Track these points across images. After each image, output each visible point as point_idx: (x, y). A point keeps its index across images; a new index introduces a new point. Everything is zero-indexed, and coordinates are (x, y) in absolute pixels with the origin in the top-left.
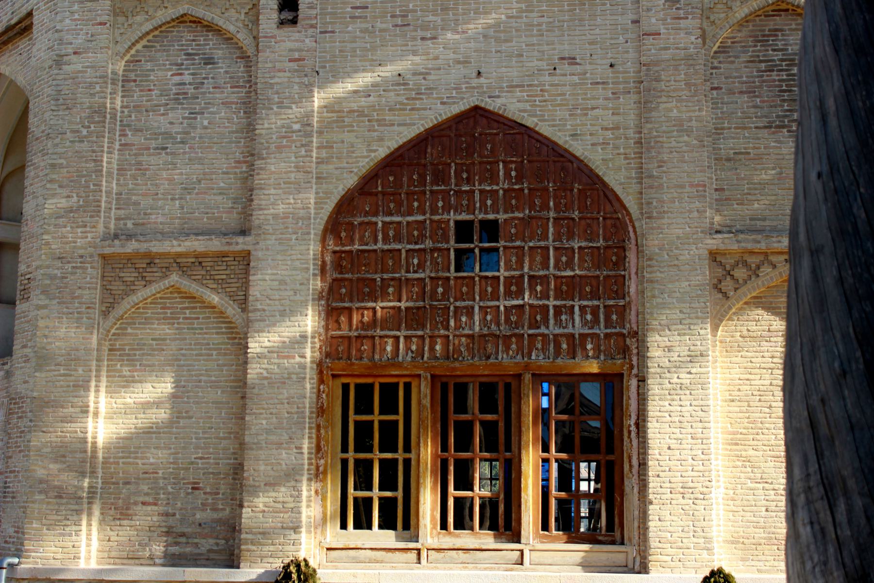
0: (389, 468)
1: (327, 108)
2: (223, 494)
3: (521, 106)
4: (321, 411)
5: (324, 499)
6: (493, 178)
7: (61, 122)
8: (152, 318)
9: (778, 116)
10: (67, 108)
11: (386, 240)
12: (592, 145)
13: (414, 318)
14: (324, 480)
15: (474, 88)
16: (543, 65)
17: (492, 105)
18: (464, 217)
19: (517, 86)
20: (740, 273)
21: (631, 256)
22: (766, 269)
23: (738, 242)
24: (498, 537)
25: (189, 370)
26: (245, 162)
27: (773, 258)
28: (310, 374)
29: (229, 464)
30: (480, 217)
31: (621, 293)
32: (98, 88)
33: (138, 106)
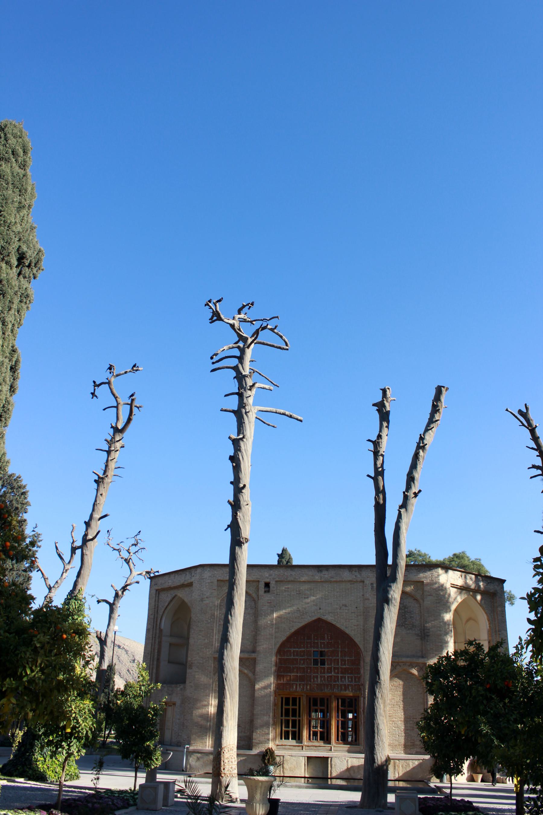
0: (294, 722)
1: (278, 617)
4: (275, 705)
5: (276, 731)
6: (323, 638)
11: (294, 656)
13: (302, 679)
14: (276, 725)
16: (338, 607)
17: (324, 618)
18: (315, 649)
21: (362, 662)
22: (398, 667)
24: (324, 743)
27: (400, 664)
28: (272, 694)
31: (359, 673)
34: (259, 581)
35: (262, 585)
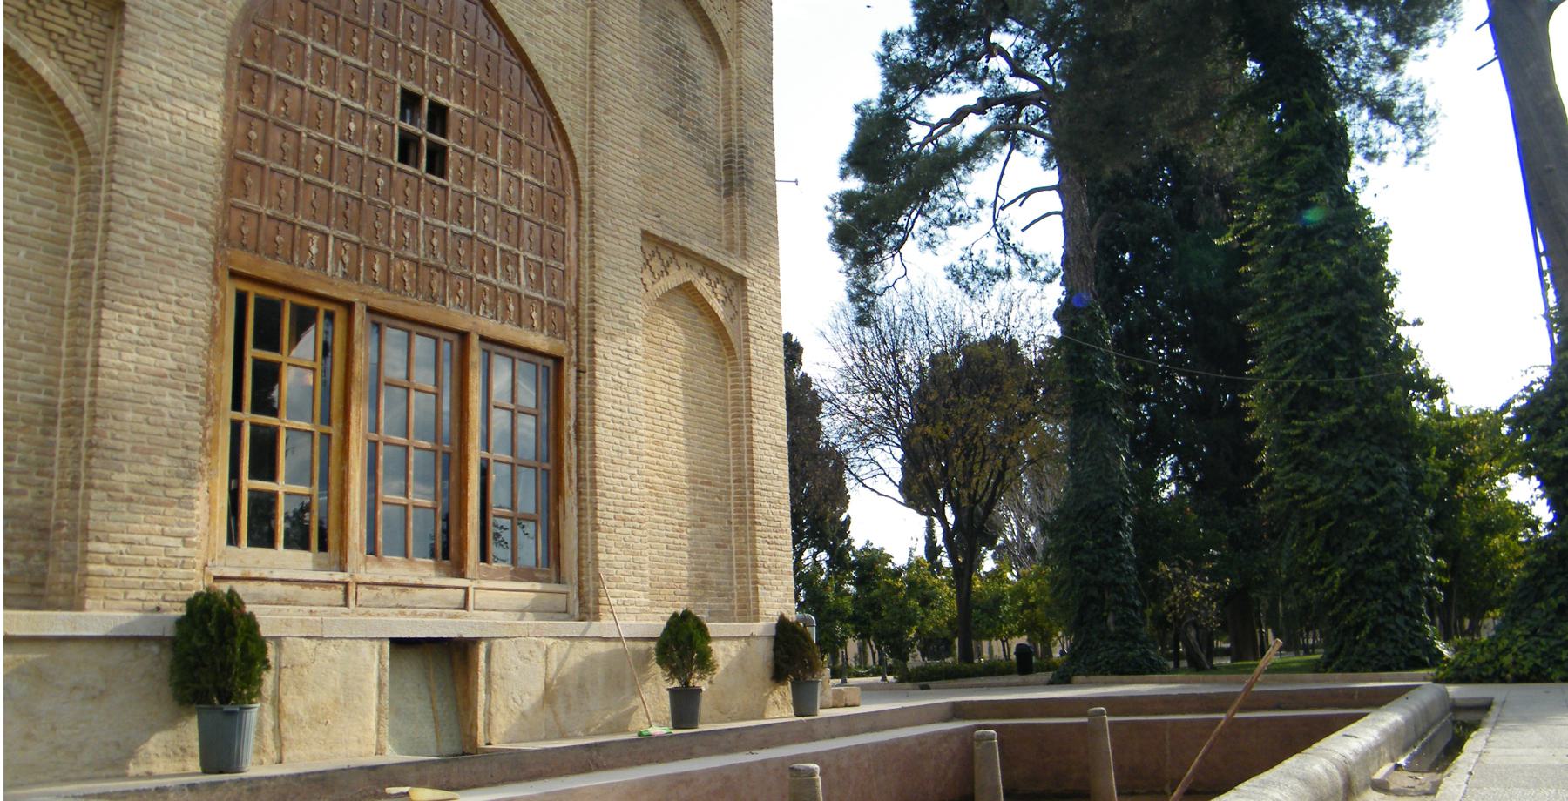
2: (22, 461)
29: (36, 402)
30: (431, 94)
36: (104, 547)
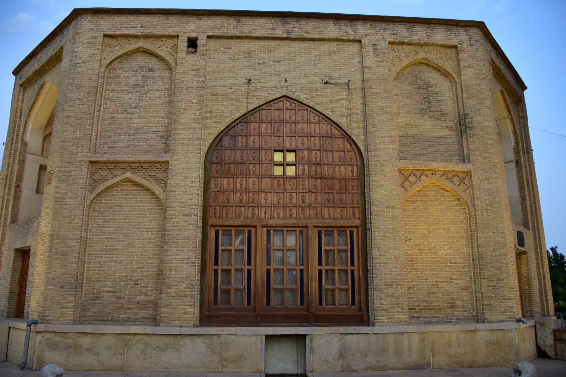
2: (151, 287)
3: (306, 96)
7: (73, 95)
8: (115, 195)
9: (423, 109)
10: (77, 89)
12: (341, 116)
15: (283, 87)
19: (304, 88)
20: (412, 179)
22: (423, 177)
23: (411, 163)
25: (134, 222)
26: (167, 118)
32: (94, 79)
33: (114, 90)
34: (177, 37)
35: (183, 43)
36: (166, 310)
